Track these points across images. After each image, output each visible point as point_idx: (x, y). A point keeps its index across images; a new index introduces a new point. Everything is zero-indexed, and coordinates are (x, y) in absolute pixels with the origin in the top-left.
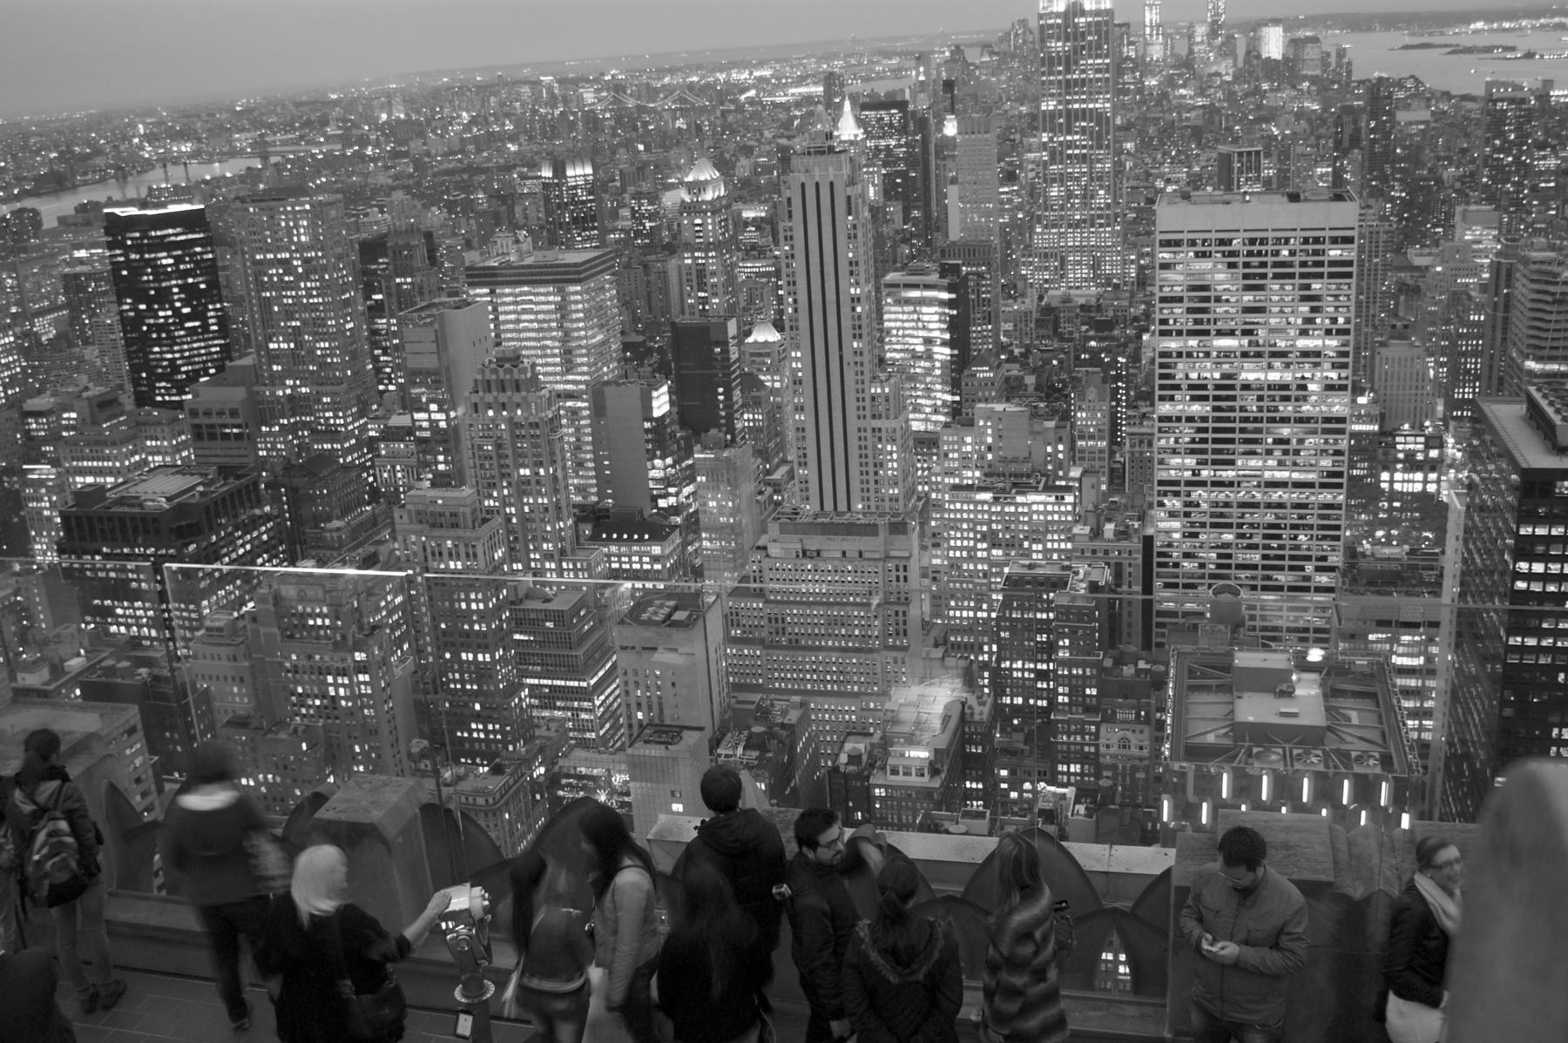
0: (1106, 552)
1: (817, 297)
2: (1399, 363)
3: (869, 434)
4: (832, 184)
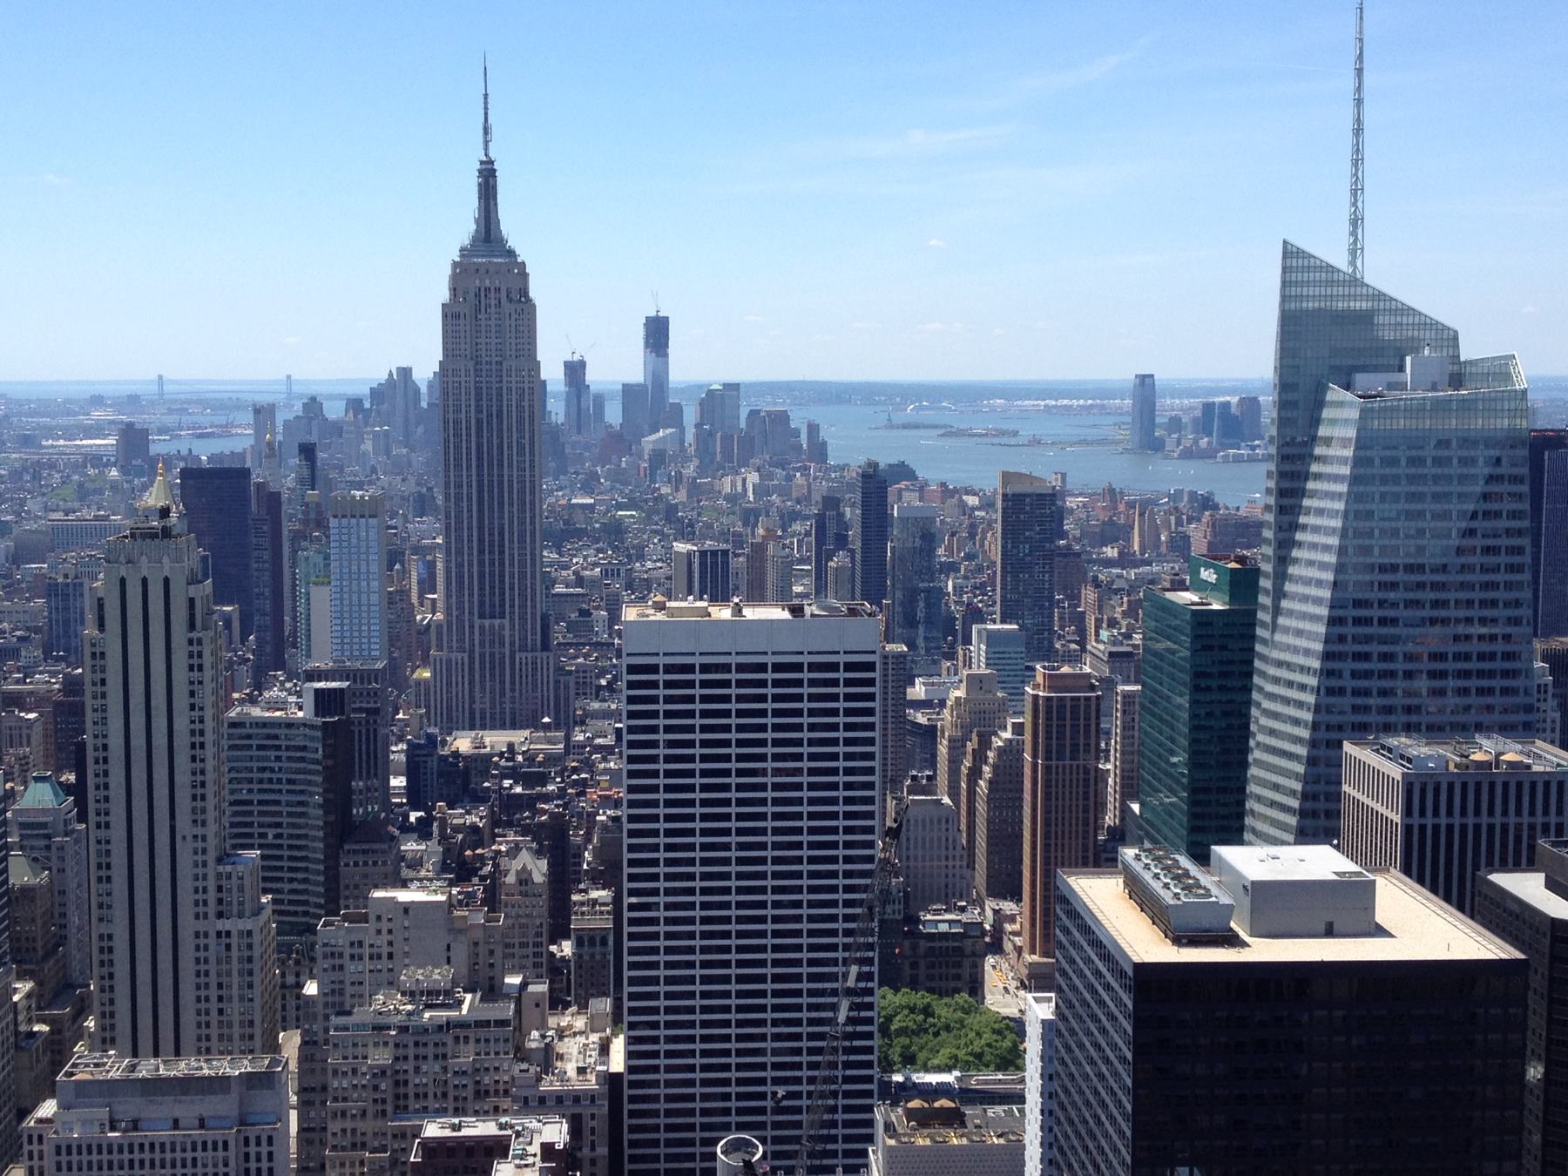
1: (138, 741)
2: (924, 826)
3: (212, 941)
4: (166, 581)
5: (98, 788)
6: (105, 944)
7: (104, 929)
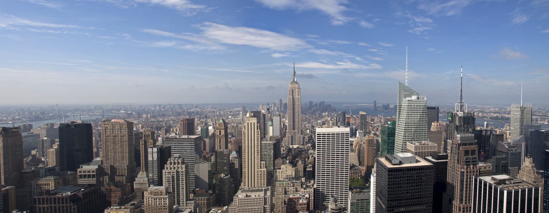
0: (307, 192)
1: (250, 145)
3: (259, 172)
5: (244, 151)
6: (244, 172)
7: (244, 170)
